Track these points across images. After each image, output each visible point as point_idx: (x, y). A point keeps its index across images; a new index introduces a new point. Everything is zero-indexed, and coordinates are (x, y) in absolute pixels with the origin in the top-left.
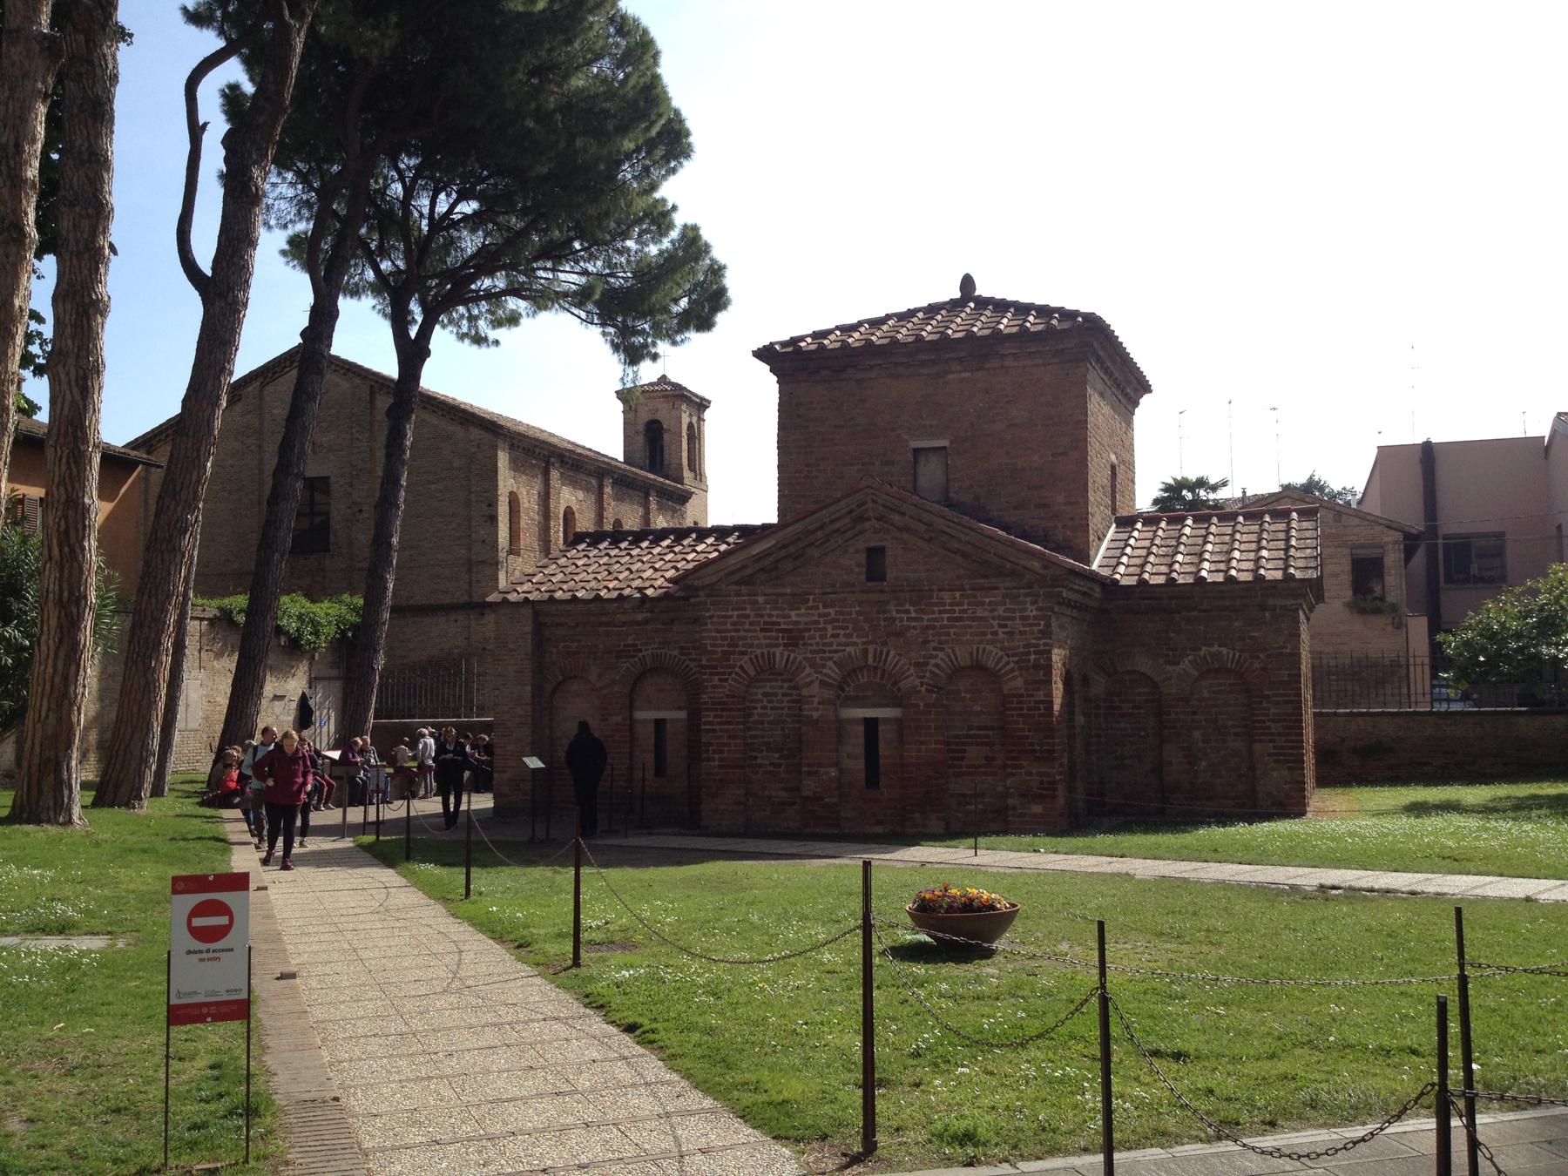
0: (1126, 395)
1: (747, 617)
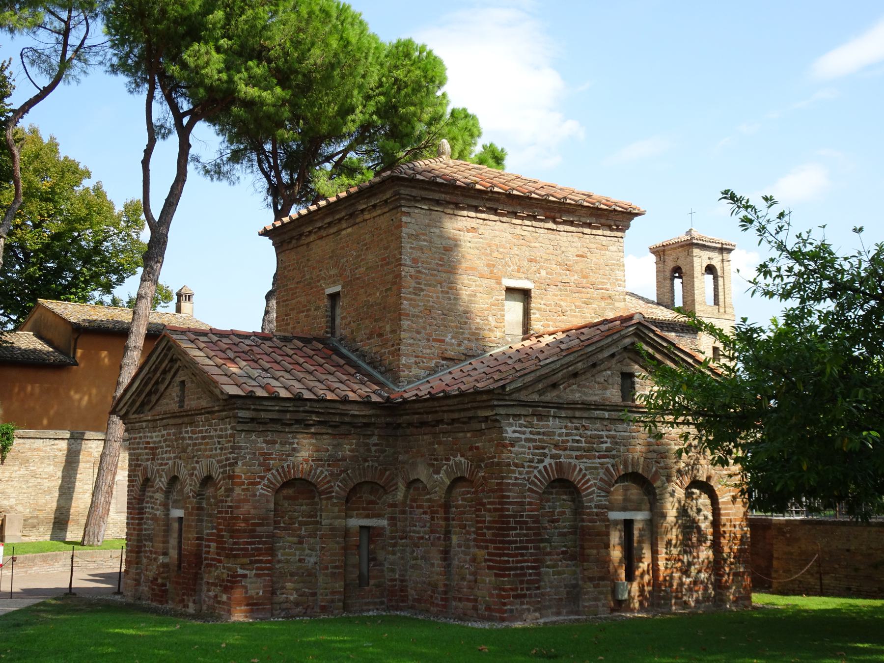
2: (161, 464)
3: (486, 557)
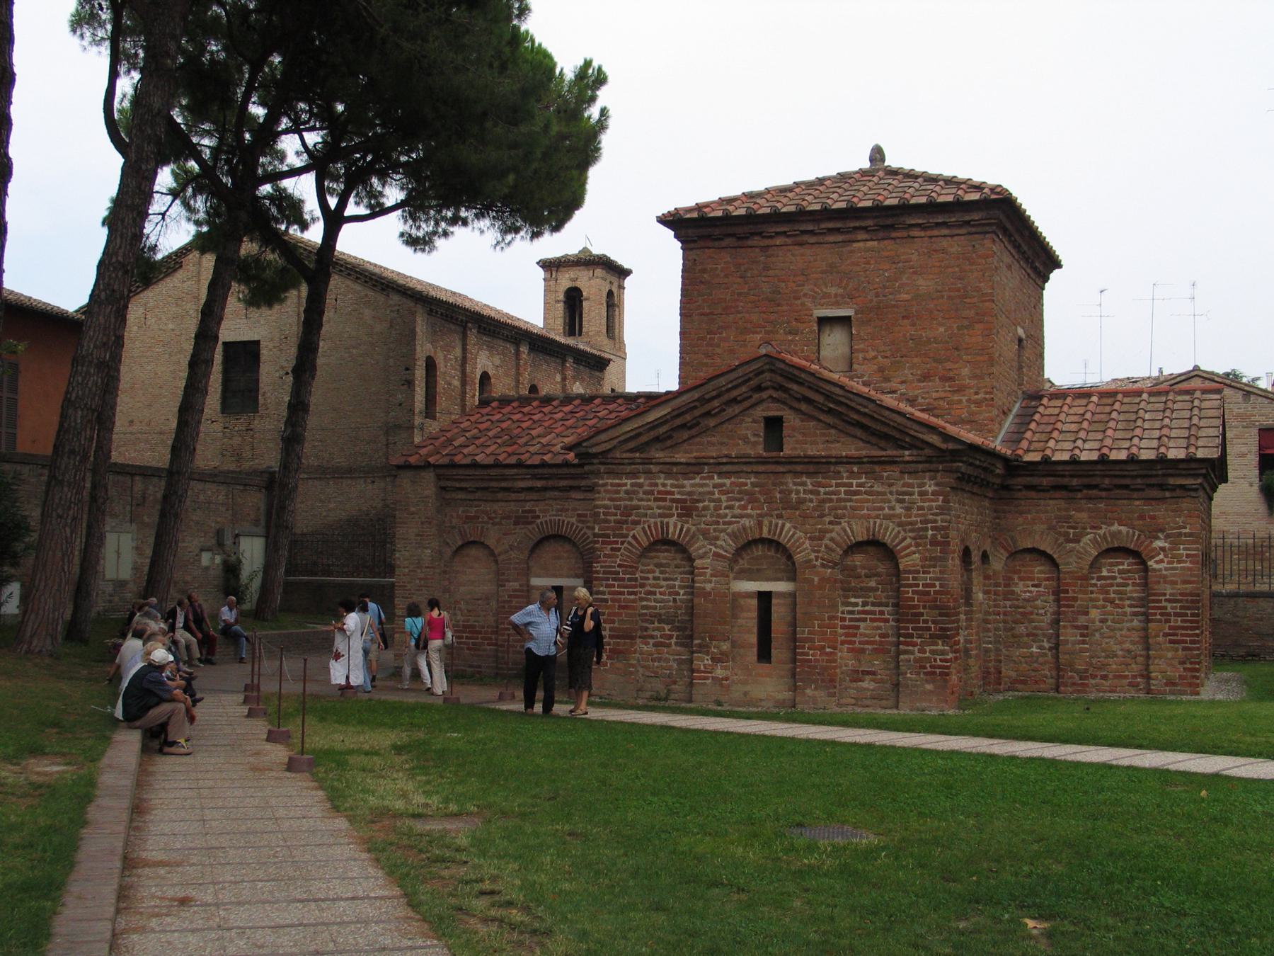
0: (1035, 269)
1: (641, 485)
2: (718, 523)
3: (1167, 631)
